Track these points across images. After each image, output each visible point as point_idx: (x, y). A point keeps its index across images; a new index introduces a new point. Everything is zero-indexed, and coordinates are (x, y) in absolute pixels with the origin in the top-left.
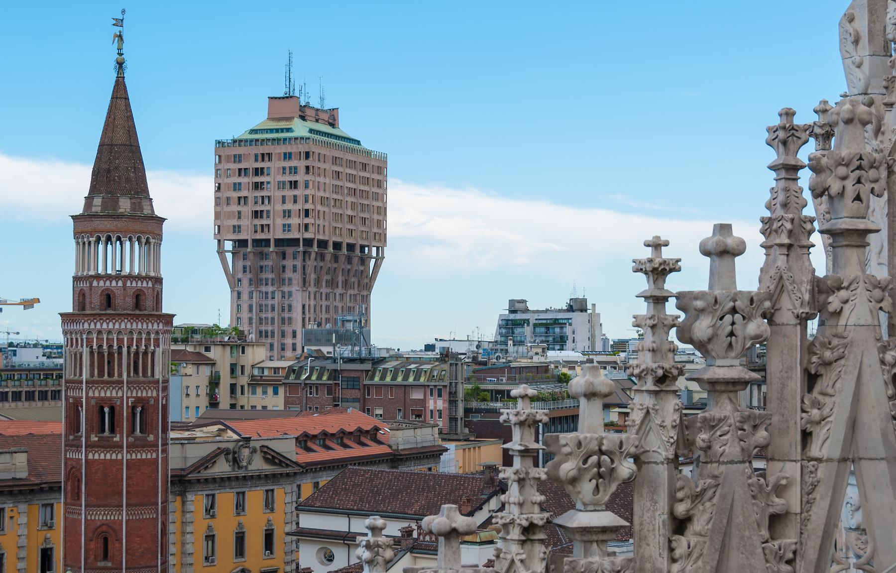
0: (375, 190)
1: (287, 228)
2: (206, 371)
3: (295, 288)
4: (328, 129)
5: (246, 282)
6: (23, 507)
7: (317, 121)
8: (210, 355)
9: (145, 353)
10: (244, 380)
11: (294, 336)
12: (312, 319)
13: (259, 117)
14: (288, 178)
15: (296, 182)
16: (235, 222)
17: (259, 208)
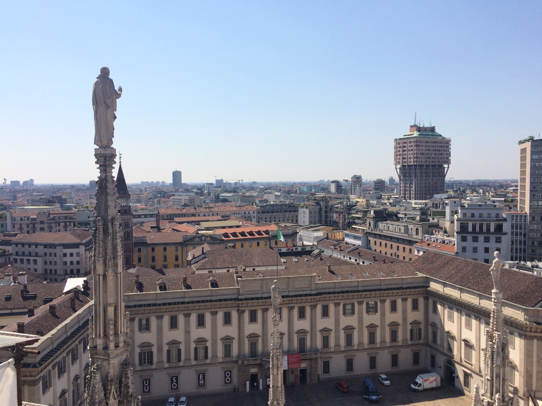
0: (445, 148)
2: (319, 207)
3: (413, 178)
4: (433, 133)
6: (145, 248)
7: (426, 131)
9: (127, 222)
11: (413, 191)
12: (419, 186)
15: (412, 149)
17: (404, 157)
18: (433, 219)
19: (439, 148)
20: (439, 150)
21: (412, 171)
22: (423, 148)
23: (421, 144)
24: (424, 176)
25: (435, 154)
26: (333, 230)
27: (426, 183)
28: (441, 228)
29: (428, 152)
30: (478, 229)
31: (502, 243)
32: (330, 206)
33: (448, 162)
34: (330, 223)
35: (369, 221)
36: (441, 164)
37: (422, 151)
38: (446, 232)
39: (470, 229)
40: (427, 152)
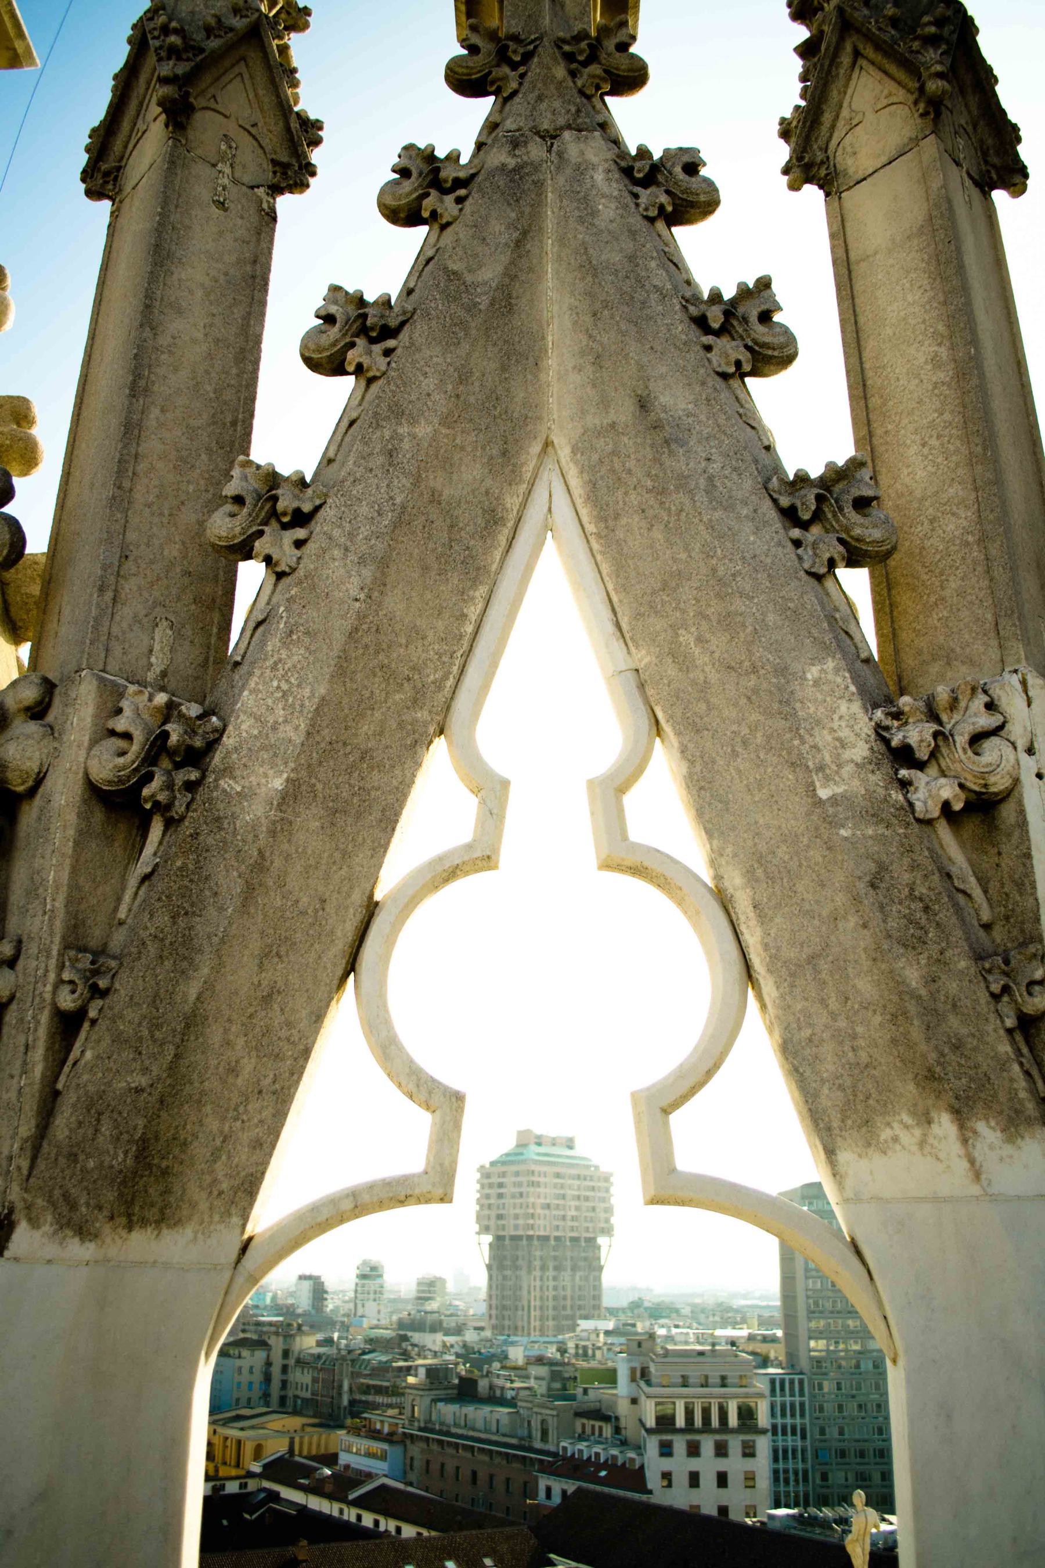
1: (516, 1227)
5: (494, 1268)
7: (554, 1145)
8: (270, 1342)
10: (291, 1362)
13: (508, 1144)
14: (517, 1190)
16: (486, 1223)
17: (501, 1212)
18: (585, 1391)
19: (588, 1193)
20: (587, 1199)
21: (520, 1253)
22: (548, 1190)
23: (542, 1180)
24: (551, 1269)
25: (577, 1208)
26: (304, 1425)
27: (555, 1288)
28: (606, 1419)
29: (561, 1202)
30: (698, 1421)
31: (756, 1459)
32: (296, 1354)
33: (608, 1231)
34: (295, 1402)
35: (411, 1397)
36: (592, 1235)
37: (546, 1197)
38: (617, 1430)
39: (680, 1422)
40: (556, 1202)
